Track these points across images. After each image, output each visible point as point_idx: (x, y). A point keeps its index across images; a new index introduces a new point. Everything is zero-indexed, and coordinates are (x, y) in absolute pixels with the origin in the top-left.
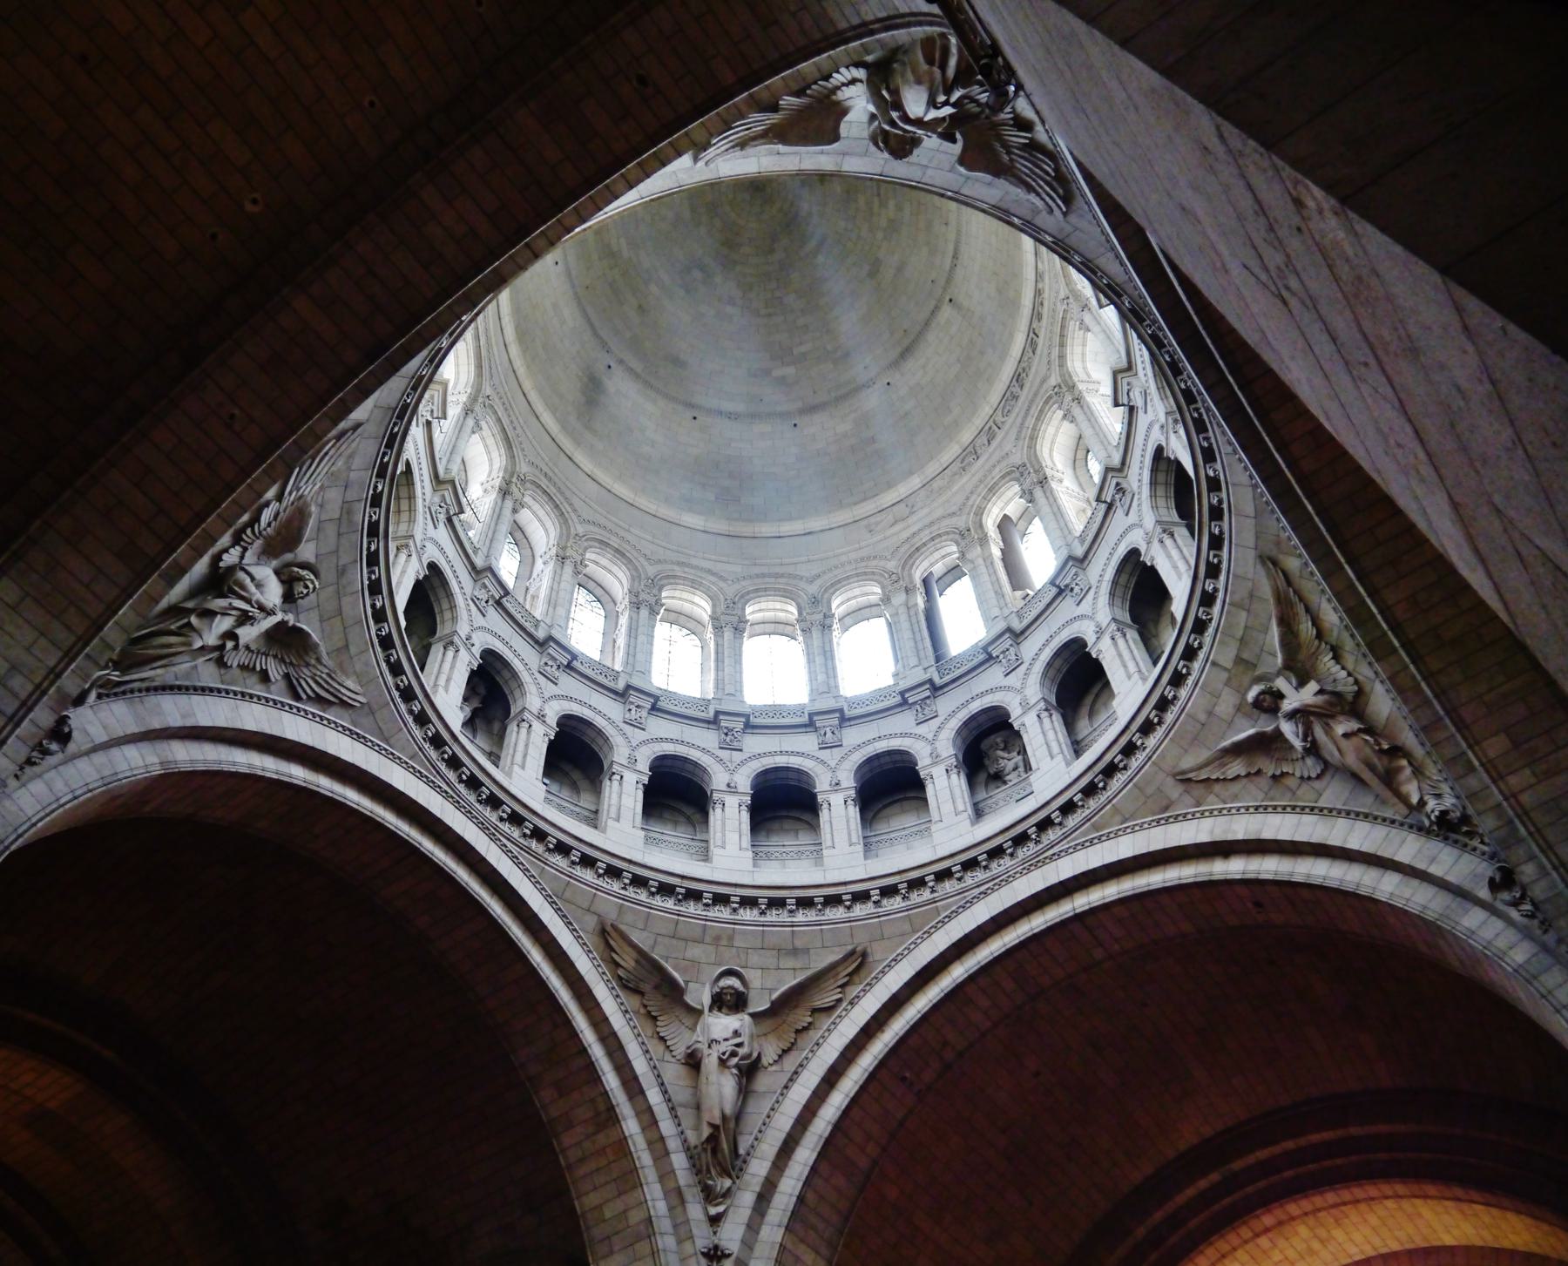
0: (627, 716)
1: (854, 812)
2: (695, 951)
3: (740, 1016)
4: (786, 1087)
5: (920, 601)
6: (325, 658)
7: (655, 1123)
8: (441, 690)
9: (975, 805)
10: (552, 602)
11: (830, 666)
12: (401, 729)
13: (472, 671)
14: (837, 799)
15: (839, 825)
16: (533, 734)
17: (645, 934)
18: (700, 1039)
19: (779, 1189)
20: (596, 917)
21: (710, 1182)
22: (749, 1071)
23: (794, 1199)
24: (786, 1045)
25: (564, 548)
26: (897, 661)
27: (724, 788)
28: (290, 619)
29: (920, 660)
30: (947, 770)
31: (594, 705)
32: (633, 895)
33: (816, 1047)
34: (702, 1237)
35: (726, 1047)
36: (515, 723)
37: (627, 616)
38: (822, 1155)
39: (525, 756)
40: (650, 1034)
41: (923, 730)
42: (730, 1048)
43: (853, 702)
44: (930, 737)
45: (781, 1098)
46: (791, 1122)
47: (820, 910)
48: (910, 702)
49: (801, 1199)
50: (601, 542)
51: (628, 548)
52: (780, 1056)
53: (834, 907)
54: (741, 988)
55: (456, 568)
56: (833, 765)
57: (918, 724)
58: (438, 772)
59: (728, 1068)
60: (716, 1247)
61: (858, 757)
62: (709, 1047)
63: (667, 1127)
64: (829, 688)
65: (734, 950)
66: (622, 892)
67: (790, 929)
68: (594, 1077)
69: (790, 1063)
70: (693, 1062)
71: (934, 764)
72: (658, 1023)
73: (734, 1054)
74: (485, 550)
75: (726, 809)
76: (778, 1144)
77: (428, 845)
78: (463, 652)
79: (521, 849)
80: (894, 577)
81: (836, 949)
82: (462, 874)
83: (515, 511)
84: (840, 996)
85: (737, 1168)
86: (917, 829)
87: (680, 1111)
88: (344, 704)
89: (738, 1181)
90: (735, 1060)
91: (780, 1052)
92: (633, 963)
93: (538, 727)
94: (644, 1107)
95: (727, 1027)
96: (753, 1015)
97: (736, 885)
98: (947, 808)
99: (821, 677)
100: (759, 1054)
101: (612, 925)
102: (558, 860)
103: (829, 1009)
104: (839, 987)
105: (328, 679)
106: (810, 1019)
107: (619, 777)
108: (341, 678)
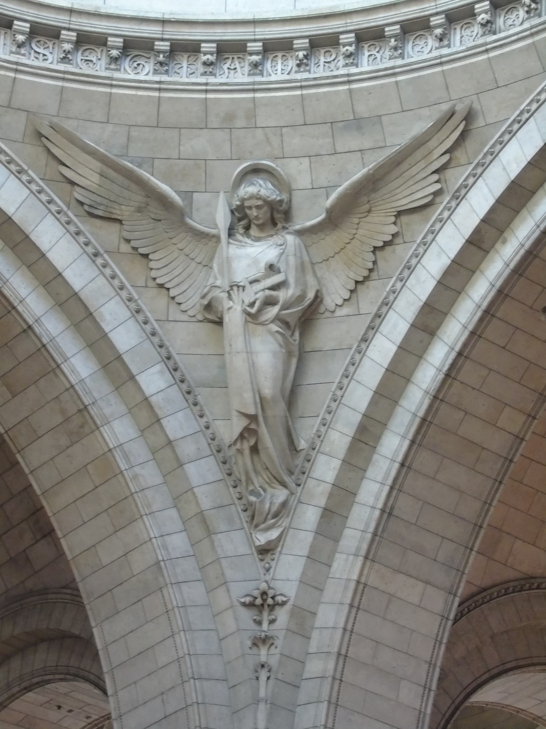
3: (277, 239)
17: (110, 128)
18: (218, 283)
21: (253, 499)
23: (377, 513)
33: (406, 273)
40: (141, 282)
42: (260, 295)
45: (358, 357)
46: (370, 394)
59: (262, 324)
65: (259, 132)
66: (62, 67)
67: (346, 87)
72: (152, 264)
73: (269, 302)
76: (351, 431)
81: (426, 112)
85: (297, 471)
90: (273, 311)
91: (352, 286)
92: (96, 178)
94: (139, 399)
95: (256, 261)
96: (300, 233)
97: (254, 22)
100: (316, 297)
104: (436, 172)
106: (394, 229)
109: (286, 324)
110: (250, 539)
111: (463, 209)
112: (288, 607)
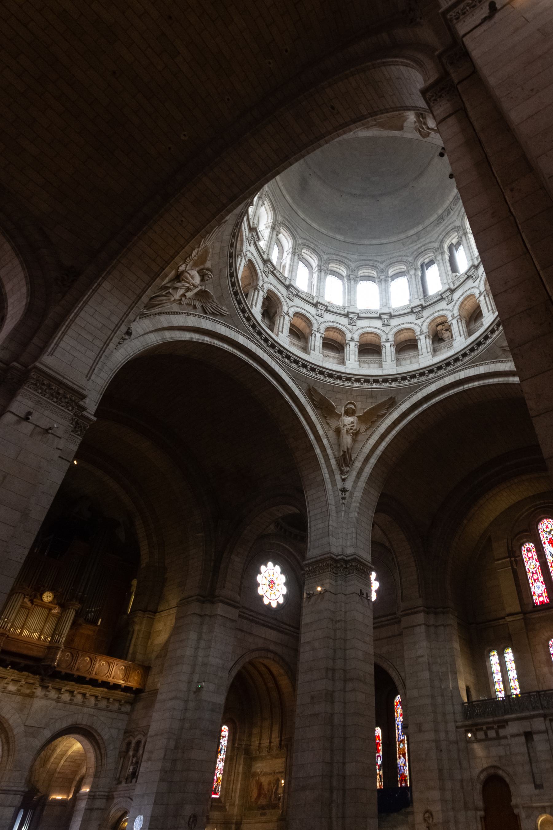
0: (317, 313)
1: (393, 349)
2: (339, 396)
3: (353, 417)
4: (367, 439)
5: (419, 273)
6: (215, 300)
7: (325, 450)
8: (254, 307)
10: (292, 270)
11: (387, 296)
13: (264, 298)
14: (388, 345)
15: (388, 354)
16: (285, 320)
19: (364, 471)
22: (356, 434)
24: (368, 426)
25: (295, 249)
26: (410, 295)
28: (203, 288)
29: (418, 296)
34: (340, 485)
35: (348, 427)
38: (378, 461)
43: (395, 310)
49: (371, 474)
50: (307, 246)
51: (317, 248)
54: (354, 408)
55: (257, 260)
56: (387, 332)
60: (344, 488)
62: (343, 427)
63: (329, 451)
64: (386, 303)
65: (352, 396)
68: (306, 436)
69: (369, 433)
70: (338, 431)
73: (351, 429)
74: (267, 252)
78: (261, 292)
80: (411, 264)
83: (277, 235)
88: (222, 315)
90: (352, 431)
93: (287, 318)
99: (384, 300)
101: (312, 387)
102: (294, 365)
106: (376, 419)
107: (314, 335)
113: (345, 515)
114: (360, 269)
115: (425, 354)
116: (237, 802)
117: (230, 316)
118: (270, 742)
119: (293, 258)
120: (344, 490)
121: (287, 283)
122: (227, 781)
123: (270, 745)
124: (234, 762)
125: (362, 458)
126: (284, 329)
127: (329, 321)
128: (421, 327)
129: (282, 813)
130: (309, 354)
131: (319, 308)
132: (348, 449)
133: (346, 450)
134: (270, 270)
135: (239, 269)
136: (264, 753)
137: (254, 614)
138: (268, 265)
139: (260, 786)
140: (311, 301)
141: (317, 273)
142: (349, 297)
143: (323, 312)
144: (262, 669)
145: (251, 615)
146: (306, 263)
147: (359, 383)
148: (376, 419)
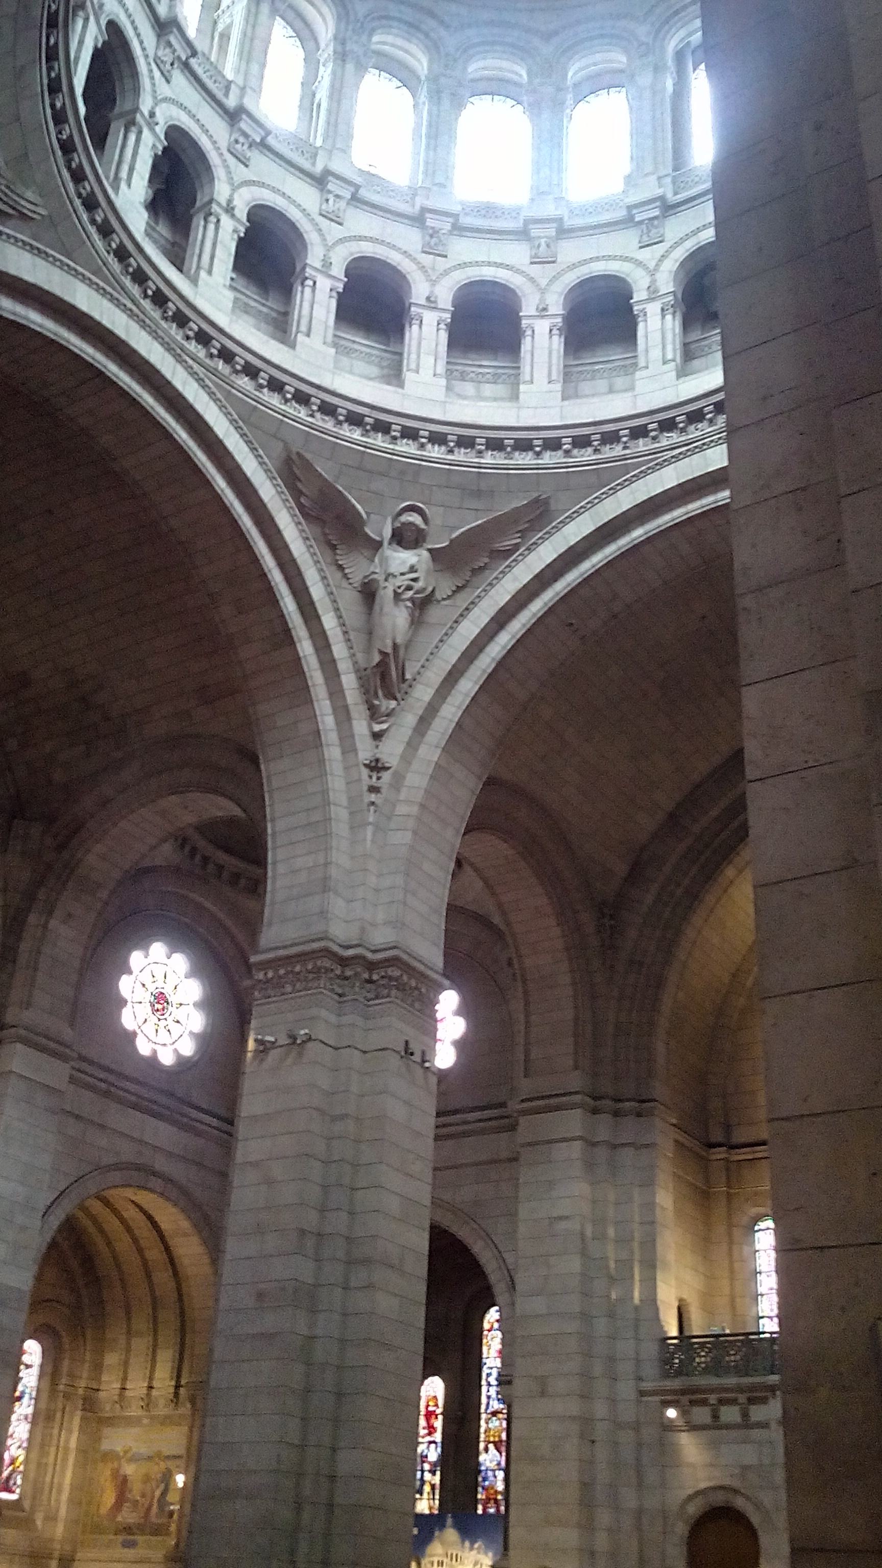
1: (558, 343)
2: (378, 484)
7: (328, 646)
8: (123, 185)
9: (685, 345)
12: (84, 243)
13: (156, 155)
14: (542, 327)
15: (541, 357)
18: (377, 571)
20: (281, 445)
21: (376, 702)
27: (423, 301)
30: (663, 310)
31: (288, 193)
32: (320, 423)
34: (365, 751)
35: (403, 581)
36: (202, 216)
37: (329, 70)
39: (212, 257)
41: (646, 255)
42: (406, 583)
44: (652, 265)
47: (509, 453)
48: (637, 219)
52: (454, 592)
53: (524, 451)
54: (423, 526)
55: (137, 22)
57: (641, 247)
58: (122, 289)
60: (377, 760)
61: (571, 278)
62: (386, 580)
63: (339, 650)
66: (310, 419)
68: (273, 600)
69: (462, 600)
71: (650, 300)
73: (409, 588)
75: (424, 327)
77: (112, 369)
79: (208, 370)
82: (147, 399)
84: (519, 540)
85: (403, 691)
86: (622, 363)
87: (352, 635)
89: (402, 702)
90: (410, 594)
91: (454, 588)
95: (404, 562)
98: (656, 354)
100: (433, 591)
101: (298, 453)
102: (244, 382)
103: (508, 553)
105: (7, 191)
106: (486, 560)
108: (20, 189)
109: (413, 603)
110: (370, 727)
111: (532, 557)
112: (389, 772)
113: (374, 834)
114: (472, 56)
115: (656, 366)
116: (63, 1512)
117: (51, 221)
118: (150, 1387)
119: (253, 10)
120: (376, 767)
121: (231, 102)
122: (39, 1464)
123: (148, 1395)
124: (57, 1426)
125: (435, 675)
126: (216, 261)
127: (361, 238)
128: (652, 273)
129: (177, 1545)
130: (292, 346)
131: (330, 192)
132: (395, 646)
133: (389, 650)
134: (179, 58)
135: (77, 58)
136: (134, 1411)
137: (111, 1078)
138: (172, 39)
139: (122, 1484)
140: (306, 165)
141: (330, 65)
142: (431, 153)
143: (342, 204)
144: (131, 1213)
145: (101, 1080)
146: (299, 24)
147: (443, 448)
148: (486, 560)
